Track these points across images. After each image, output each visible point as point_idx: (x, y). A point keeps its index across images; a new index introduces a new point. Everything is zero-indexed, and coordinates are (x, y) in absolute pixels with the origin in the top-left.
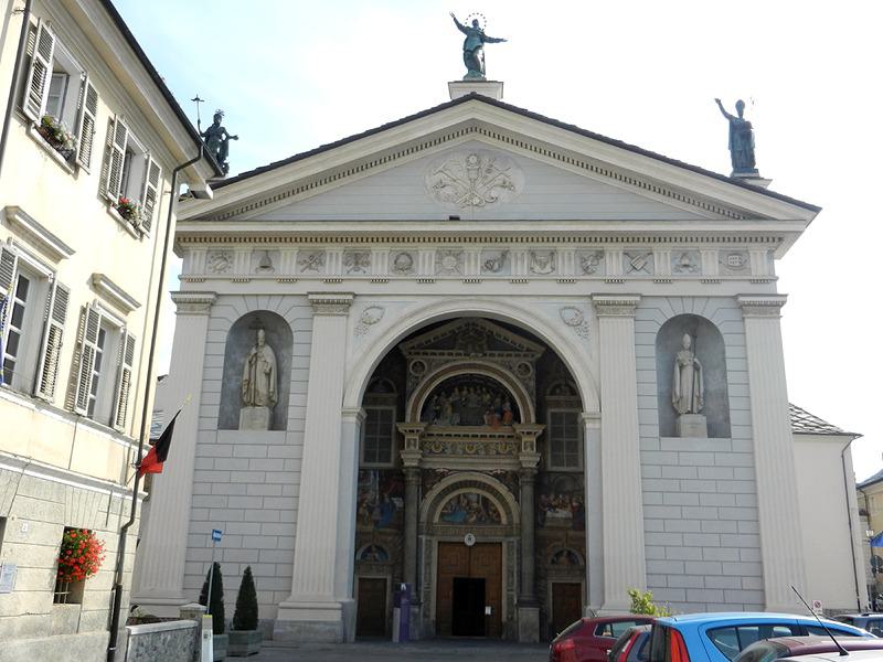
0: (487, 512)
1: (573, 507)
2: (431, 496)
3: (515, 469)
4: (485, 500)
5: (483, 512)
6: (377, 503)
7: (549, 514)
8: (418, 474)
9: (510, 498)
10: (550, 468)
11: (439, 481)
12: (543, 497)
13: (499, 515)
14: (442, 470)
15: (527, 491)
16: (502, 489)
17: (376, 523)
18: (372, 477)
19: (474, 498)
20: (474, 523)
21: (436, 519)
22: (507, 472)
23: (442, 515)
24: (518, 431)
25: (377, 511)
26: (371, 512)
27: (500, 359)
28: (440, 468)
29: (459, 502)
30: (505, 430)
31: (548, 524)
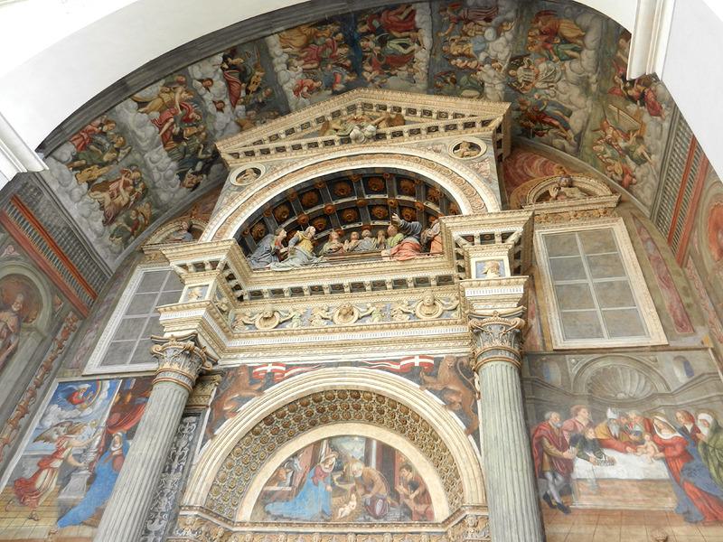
0: (394, 494)
1: (663, 446)
2: (232, 430)
3: (462, 350)
4: (387, 454)
5: (381, 488)
6: (91, 456)
7: (582, 468)
8: (189, 354)
9: (449, 427)
10: (560, 343)
11: (260, 391)
12: (553, 418)
13: (425, 497)
14: (269, 368)
15: (497, 379)
16: (426, 404)
17: (64, 510)
18: (104, 395)
19: (355, 449)
20: (351, 520)
21: (246, 511)
22: (438, 361)
23: (265, 498)
24: (456, 235)
25: (78, 481)
26: (66, 476)
27: (415, 140)
28: (263, 362)
29: (315, 460)
30: (433, 266)
31: (583, 501)
